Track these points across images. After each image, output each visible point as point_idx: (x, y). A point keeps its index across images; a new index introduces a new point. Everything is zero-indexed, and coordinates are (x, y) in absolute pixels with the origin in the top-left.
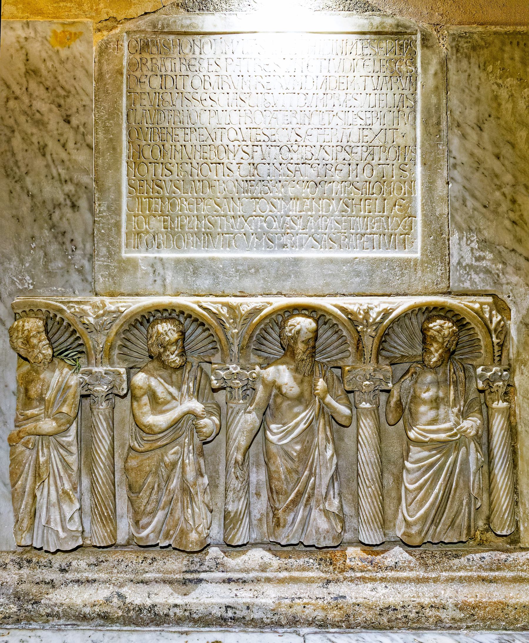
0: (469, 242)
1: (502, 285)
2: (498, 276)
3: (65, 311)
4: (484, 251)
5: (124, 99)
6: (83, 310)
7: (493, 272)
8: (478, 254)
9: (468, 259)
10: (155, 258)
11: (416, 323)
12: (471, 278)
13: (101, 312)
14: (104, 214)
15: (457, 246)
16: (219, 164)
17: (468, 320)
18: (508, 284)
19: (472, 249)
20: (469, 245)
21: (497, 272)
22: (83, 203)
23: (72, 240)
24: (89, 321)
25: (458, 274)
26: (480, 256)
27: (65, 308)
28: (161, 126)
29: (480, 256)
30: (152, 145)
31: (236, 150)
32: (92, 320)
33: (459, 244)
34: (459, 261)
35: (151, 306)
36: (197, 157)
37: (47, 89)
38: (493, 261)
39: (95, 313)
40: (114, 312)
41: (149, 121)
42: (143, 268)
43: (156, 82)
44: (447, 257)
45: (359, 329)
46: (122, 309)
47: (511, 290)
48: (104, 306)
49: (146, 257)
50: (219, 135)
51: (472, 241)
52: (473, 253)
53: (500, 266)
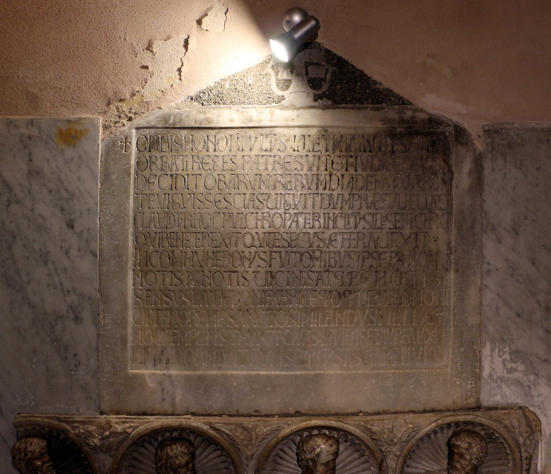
0: (501, 354)
1: (533, 397)
2: (530, 387)
3: (69, 431)
4: (516, 363)
5: (131, 201)
6: (88, 431)
7: (525, 384)
8: (509, 365)
9: (500, 371)
10: (164, 375)
11: (442, 438)
12: (502, 391)
13: (107, 433)
14: (109, 327)
15: (489, 358)
16: (234, 272)
17: (497, 435)
18: (539, 396)
19: (504, 361)
20: (501, 356)
21: (529, 383)
22: (86, 316)
23: (75, 355)
24: (94, 443)
25: (488, 387)
26: (512, 368)
27: (68, 427)
28: (171, 230)
29: (512, 368)
30: (160, 251)
31: (252, 257)
32: (96, 441)
33: (491, 356)
34: (490, 373)
35: (160, 427)
36: (210, 265)
37: (50, 191)
38: (526, 373)
39: (101, 434)
40: (121, 433)
41: (158, 226)
42: (151, 385)
43: (166, 182)
44: (478, 370)
45: (383, 449)
46: (129, 430)
47: (542, 403)
48: (110, 427)
49: (153, 374)
50: (234, 239)
51: (504, 353)
52: (505, 365)
53: (532, 377)
